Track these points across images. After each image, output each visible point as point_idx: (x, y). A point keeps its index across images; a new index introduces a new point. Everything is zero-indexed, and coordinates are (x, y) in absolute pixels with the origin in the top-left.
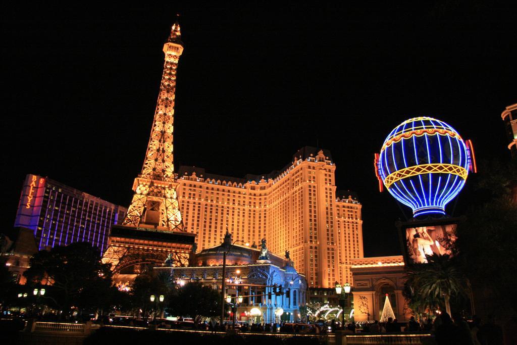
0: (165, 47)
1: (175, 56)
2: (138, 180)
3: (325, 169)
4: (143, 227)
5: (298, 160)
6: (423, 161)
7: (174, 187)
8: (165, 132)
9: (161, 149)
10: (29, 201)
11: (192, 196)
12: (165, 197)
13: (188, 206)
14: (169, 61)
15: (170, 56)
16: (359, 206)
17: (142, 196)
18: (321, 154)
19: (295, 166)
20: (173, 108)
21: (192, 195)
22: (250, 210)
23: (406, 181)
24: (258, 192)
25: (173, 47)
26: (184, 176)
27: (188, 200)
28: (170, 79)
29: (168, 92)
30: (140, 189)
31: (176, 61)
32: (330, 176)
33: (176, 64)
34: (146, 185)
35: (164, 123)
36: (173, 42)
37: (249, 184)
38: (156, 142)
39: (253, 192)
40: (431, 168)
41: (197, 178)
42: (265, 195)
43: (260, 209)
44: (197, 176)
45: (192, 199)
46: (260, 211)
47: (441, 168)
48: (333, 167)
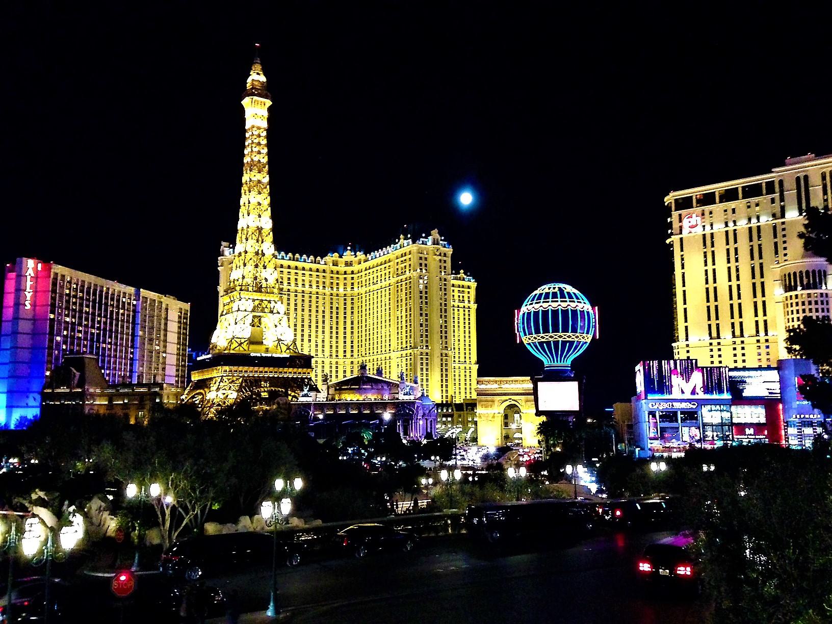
3: (440, 255)
4: (244, 349)
6: (556, 330)
8: (262, 229)
10: (28, 298)
16: (473, 284)
18: (435, 233)
22: (332, 295)
23: (541, 344)
24: (342, 268)
31: (265, 124)
32: (445, 261)
36: (259, 95)
37: (329, 258)
38: (252, 242)
39: (335, 268)
40: (561, 336)
47: (569, 337)
48: (449, 251)
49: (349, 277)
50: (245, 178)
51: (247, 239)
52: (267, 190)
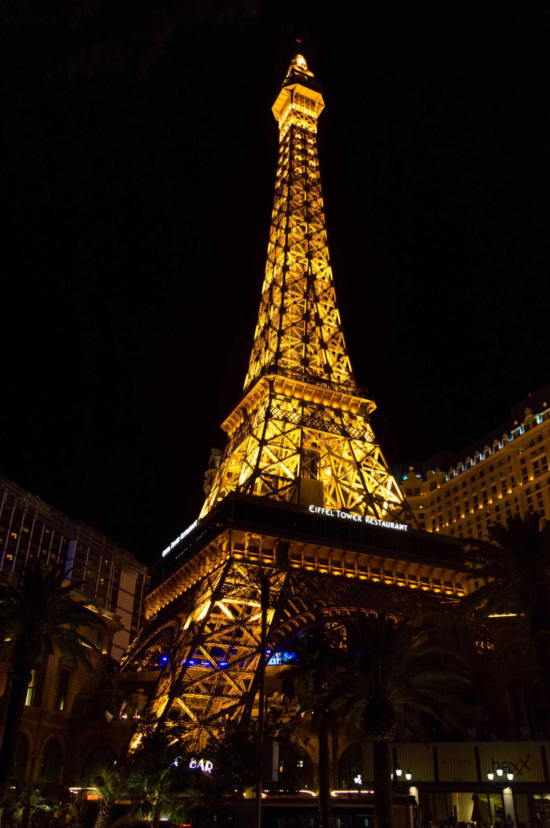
0: (284, 95)
2: (271, 382)
5: (534, 414)
14: (299, 125)
15: (299, 116)
17: (289, 426)
19: (527, 429)
25: (302, 97)
29: (307, 188)
31: (313, 129)
34: (293, 397)
35: (310, 256)
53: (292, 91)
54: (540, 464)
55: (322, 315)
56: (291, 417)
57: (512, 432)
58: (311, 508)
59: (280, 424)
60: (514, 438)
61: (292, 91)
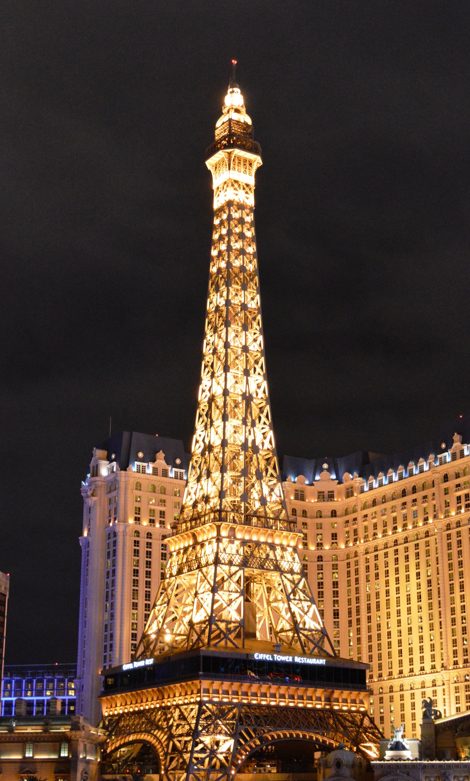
1: (247, 185)
2: (218, 527)
7: (293, 543)
9: (250, 445)
11: (157, 519)
12: (277, 568)
13: (149, 545)
14: (237, 199)
15: (236, 186)
17: (234, 569)
19: (454, 458)
20: (261, 334)
21: (157, 514)
25: (239, 158)
26: (136, 463)
27: (151, 530)
28: (242, 252)
30: (225, 550)
31: (250, 201)
33: (251, 209)
35: (246, 373)
41: (169, 468)
42: (334, 514)
43: (320, 553)
44: (168, 464)
45: (158, 525)
46: (320, 558)
49: (327, 521)
50: (215, 300)
51: (225, 418)
52: (256, 327)
53: (230, 154)
54: (463, 499)
55: (258, 443)
56: (235, 560)
57: (439, 456)
58: (256, 655)
59: (226, 568)
60: (441, 464)
61: (230, 154)
